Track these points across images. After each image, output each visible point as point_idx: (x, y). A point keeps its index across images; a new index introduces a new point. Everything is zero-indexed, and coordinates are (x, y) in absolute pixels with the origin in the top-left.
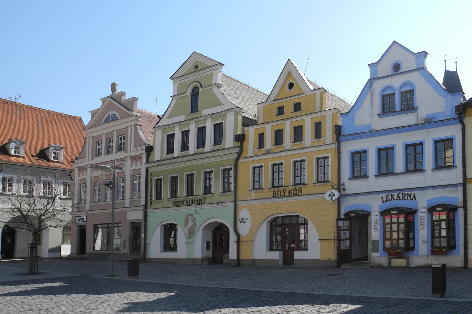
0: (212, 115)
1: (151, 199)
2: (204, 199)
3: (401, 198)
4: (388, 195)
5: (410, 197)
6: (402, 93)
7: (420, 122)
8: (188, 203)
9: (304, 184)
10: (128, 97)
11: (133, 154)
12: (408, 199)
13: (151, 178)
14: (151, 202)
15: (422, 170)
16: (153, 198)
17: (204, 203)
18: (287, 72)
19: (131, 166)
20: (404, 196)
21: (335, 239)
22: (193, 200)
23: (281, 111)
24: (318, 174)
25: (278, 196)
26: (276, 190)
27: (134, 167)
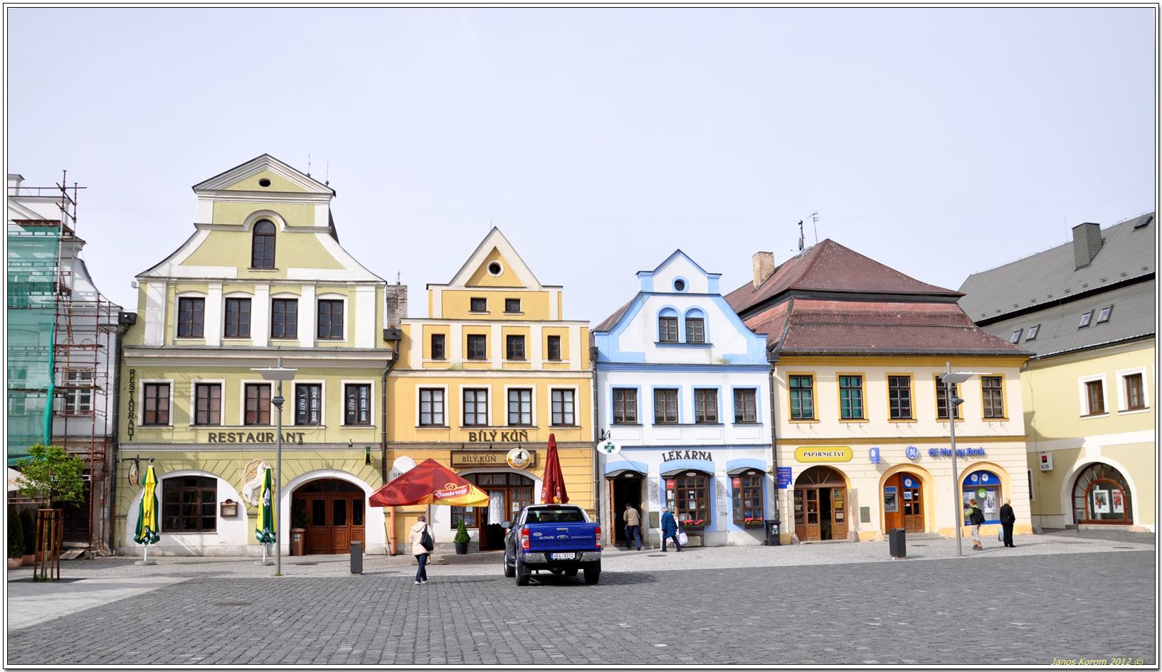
0: (317, 284)
1: (131, 422)
2: (301, 435)
3: (691, 456)
5: (704, 456)
7: (714, 363)
8: (252, 438)
12: (700, 459)
13: (132, 379)
16: (139, 421)
20: (695, 454)
22: (267, 434)
23: (478, 304)
25: (480, 440)
26: (476, 431)
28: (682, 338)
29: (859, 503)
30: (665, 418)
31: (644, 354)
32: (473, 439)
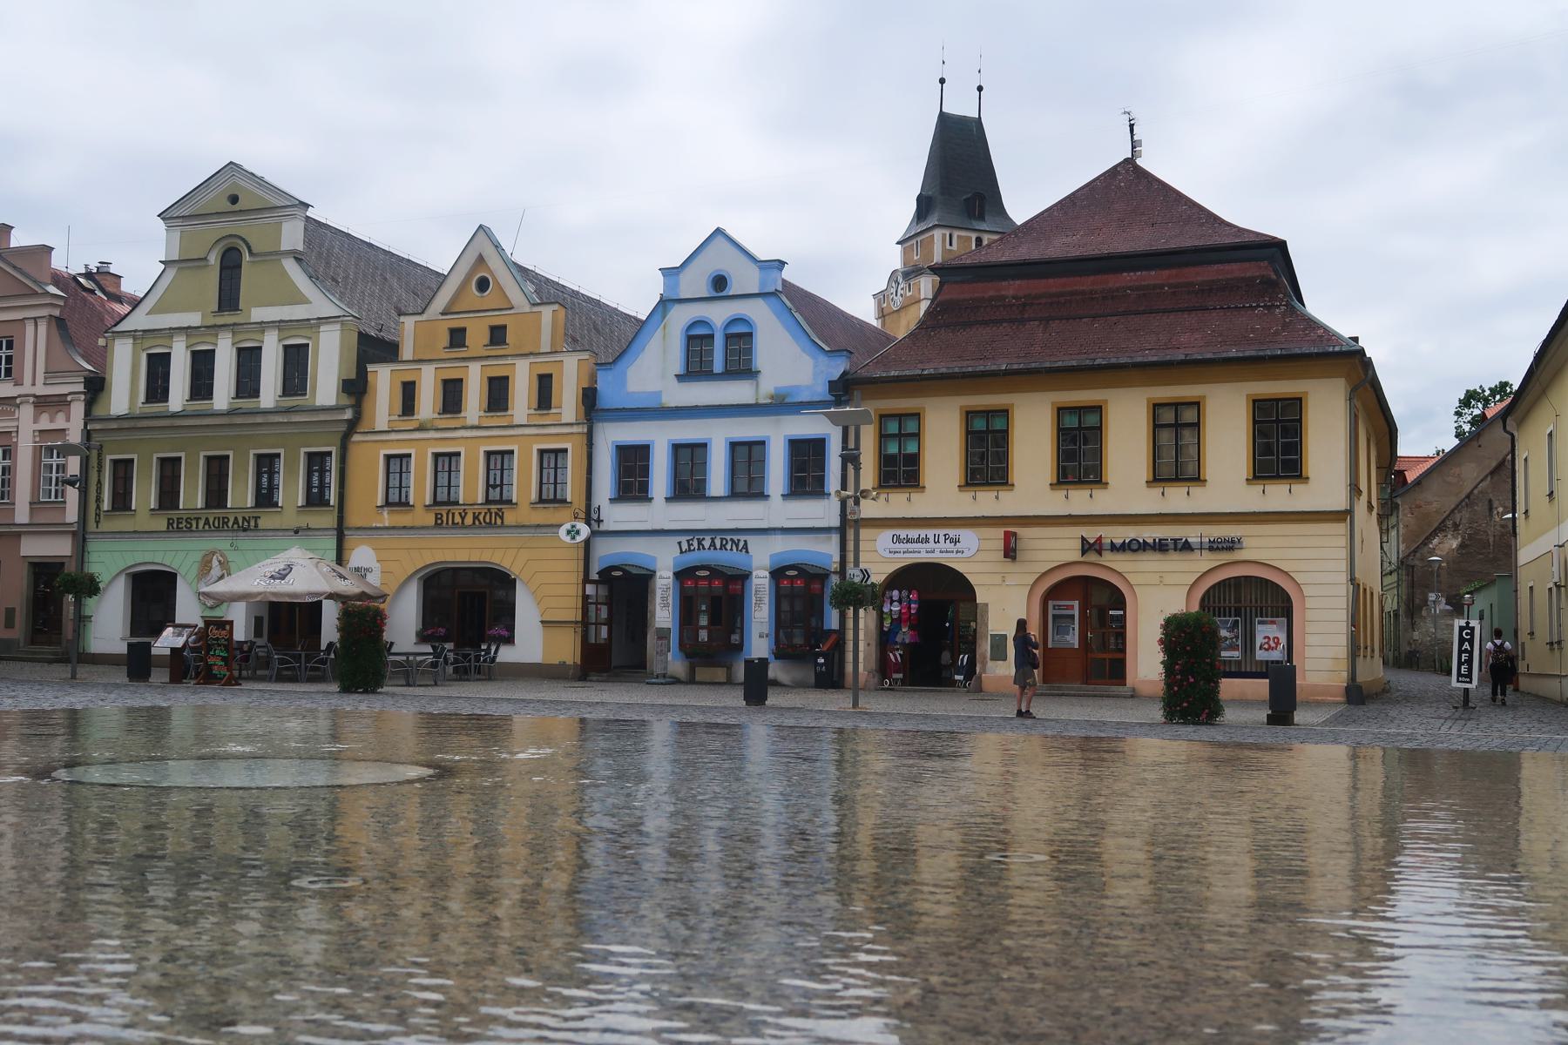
0: (280, 325)
1: (98, 507)
3: (718, 546)
4: (692, 540)
5: (737, 546)
6: (729, 337)
7: (762, 401)
9: (509, 502)
10: (18, 240)
11: (41, 390)
12: (731, 549)
14: (98, 515)
15: (761, 496)
16: (106, 505)
17: (256, 526)
18: (476, 255)
19: (35, 422)
21: (576, 622)
22: (223, 518)
23: (457, 337)
24: (541, 483)
25: (447, 523)
26: (443, 510)
27: (45, 423)
29: (989, 628)
30: (688, 487)
31: (658, 394)
32: (439, 522)
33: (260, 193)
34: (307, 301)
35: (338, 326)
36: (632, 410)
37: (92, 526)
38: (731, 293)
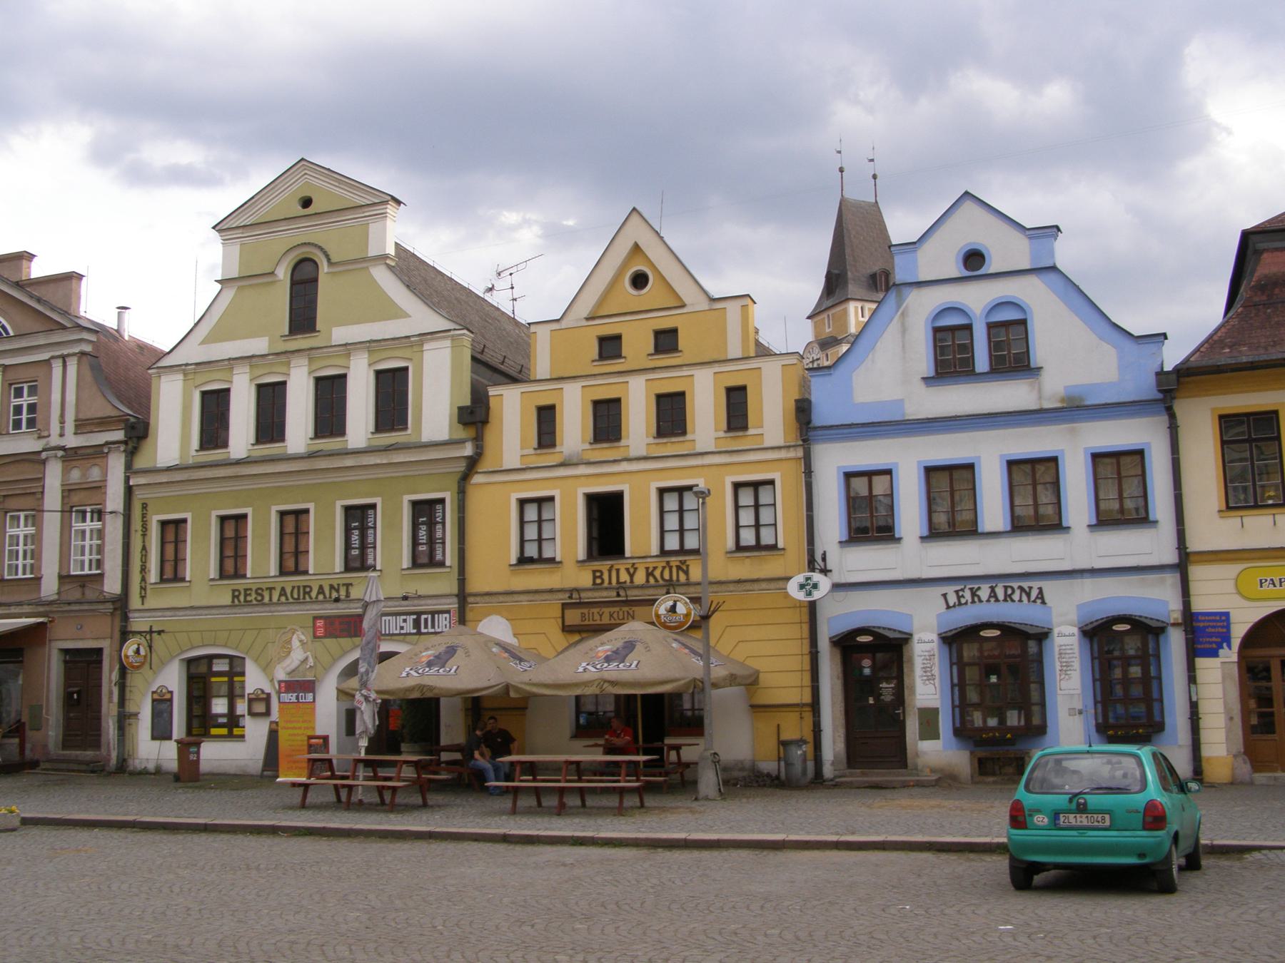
0: (371, 346)
1: (143, 579)
2: (348, 585)
3: (1001, 595)
4: (962, 590)
5: (1028, 595)
6: (991, 327)
7: (1047, 405)
8: (285, 595)
10: (37, 270)
11: (72, 441)
12: (1020, 601)
13: (144, 516)
14: (143, 588)
15: (1056, 525)
16: (153, 576)
17: (348, 595)
18: (630, 245)
20: (1009, 591)
23: (610, 346)
25: (610, 582)
28: (982, 362)
32: (598, 581)
33: (338, 191)
34: (406, 315)
35: (448, 343)
36: (864, 425)
37: (135, 602)
38: (991, 271)
